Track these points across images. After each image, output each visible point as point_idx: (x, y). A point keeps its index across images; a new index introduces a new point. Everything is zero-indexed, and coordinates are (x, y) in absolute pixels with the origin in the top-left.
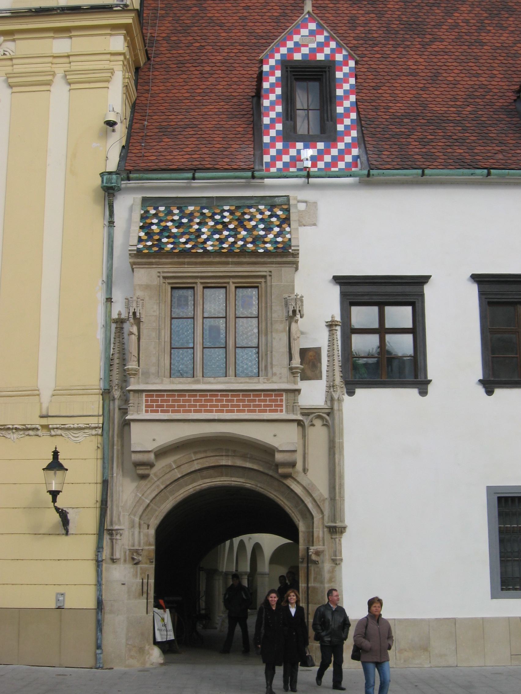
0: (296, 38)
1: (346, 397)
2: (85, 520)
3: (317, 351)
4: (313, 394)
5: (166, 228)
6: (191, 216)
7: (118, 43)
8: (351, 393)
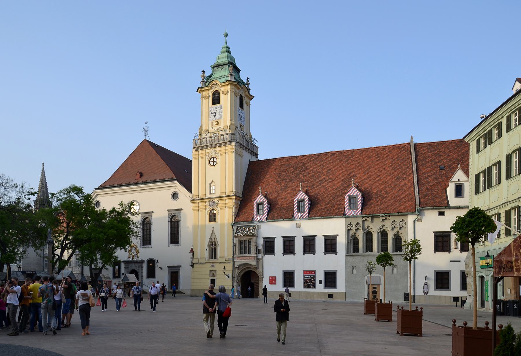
2: (231, 276)
4: (260, 256)
7: (234, 201)
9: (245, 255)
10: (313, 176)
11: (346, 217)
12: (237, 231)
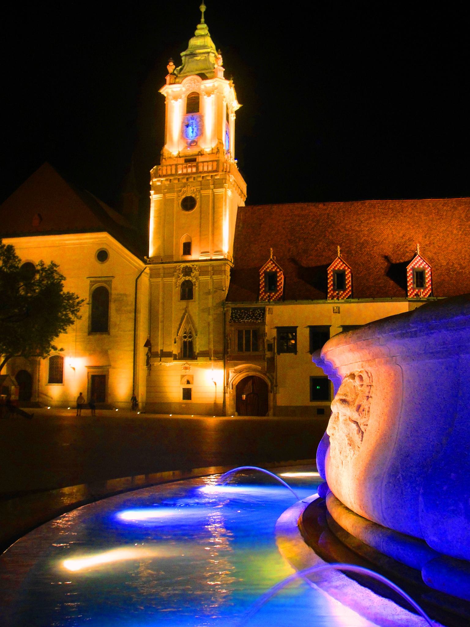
0: (268, 265)
1: (278, 357)
3: (272, 344)
5: (236, 317)
6: (242, 313)
8: (279, 354)
9: (248, 353)
10: (348, 235)
11: (409, 301)
12: (232, 316)
